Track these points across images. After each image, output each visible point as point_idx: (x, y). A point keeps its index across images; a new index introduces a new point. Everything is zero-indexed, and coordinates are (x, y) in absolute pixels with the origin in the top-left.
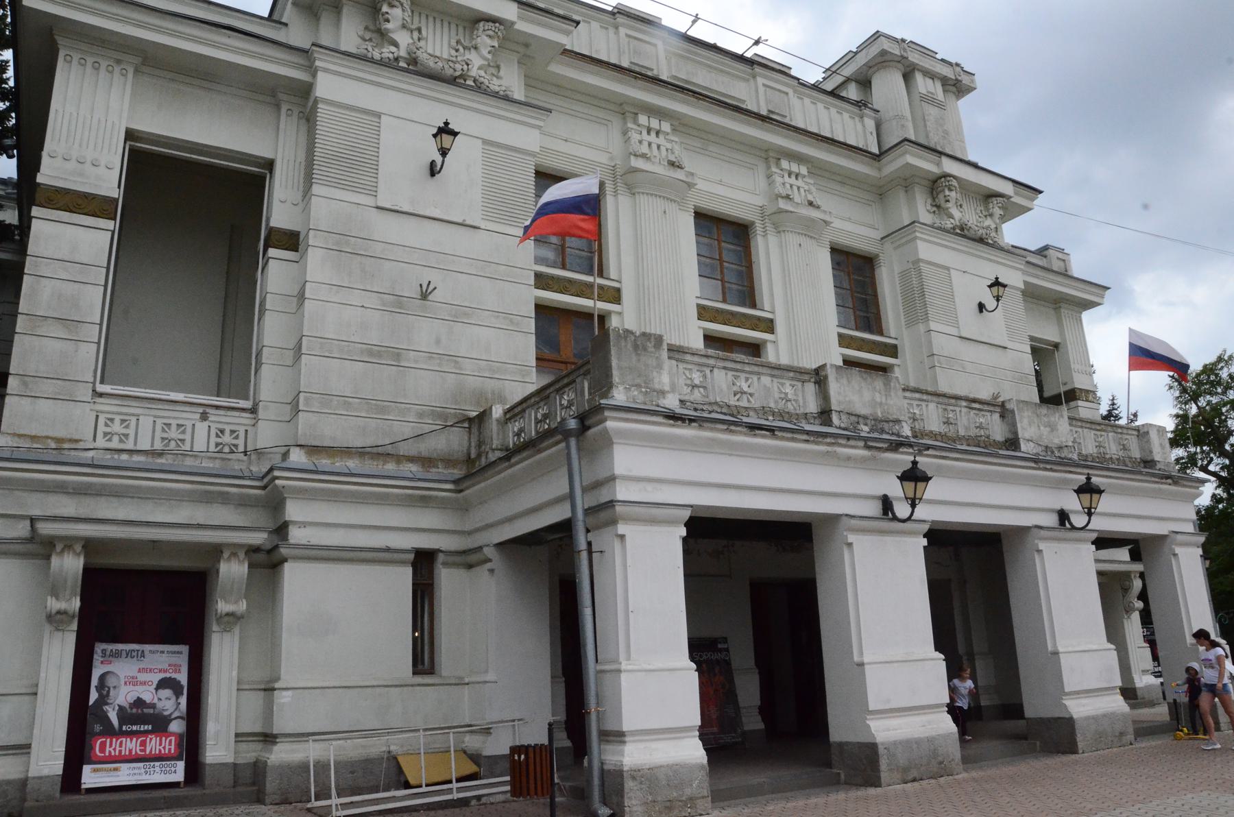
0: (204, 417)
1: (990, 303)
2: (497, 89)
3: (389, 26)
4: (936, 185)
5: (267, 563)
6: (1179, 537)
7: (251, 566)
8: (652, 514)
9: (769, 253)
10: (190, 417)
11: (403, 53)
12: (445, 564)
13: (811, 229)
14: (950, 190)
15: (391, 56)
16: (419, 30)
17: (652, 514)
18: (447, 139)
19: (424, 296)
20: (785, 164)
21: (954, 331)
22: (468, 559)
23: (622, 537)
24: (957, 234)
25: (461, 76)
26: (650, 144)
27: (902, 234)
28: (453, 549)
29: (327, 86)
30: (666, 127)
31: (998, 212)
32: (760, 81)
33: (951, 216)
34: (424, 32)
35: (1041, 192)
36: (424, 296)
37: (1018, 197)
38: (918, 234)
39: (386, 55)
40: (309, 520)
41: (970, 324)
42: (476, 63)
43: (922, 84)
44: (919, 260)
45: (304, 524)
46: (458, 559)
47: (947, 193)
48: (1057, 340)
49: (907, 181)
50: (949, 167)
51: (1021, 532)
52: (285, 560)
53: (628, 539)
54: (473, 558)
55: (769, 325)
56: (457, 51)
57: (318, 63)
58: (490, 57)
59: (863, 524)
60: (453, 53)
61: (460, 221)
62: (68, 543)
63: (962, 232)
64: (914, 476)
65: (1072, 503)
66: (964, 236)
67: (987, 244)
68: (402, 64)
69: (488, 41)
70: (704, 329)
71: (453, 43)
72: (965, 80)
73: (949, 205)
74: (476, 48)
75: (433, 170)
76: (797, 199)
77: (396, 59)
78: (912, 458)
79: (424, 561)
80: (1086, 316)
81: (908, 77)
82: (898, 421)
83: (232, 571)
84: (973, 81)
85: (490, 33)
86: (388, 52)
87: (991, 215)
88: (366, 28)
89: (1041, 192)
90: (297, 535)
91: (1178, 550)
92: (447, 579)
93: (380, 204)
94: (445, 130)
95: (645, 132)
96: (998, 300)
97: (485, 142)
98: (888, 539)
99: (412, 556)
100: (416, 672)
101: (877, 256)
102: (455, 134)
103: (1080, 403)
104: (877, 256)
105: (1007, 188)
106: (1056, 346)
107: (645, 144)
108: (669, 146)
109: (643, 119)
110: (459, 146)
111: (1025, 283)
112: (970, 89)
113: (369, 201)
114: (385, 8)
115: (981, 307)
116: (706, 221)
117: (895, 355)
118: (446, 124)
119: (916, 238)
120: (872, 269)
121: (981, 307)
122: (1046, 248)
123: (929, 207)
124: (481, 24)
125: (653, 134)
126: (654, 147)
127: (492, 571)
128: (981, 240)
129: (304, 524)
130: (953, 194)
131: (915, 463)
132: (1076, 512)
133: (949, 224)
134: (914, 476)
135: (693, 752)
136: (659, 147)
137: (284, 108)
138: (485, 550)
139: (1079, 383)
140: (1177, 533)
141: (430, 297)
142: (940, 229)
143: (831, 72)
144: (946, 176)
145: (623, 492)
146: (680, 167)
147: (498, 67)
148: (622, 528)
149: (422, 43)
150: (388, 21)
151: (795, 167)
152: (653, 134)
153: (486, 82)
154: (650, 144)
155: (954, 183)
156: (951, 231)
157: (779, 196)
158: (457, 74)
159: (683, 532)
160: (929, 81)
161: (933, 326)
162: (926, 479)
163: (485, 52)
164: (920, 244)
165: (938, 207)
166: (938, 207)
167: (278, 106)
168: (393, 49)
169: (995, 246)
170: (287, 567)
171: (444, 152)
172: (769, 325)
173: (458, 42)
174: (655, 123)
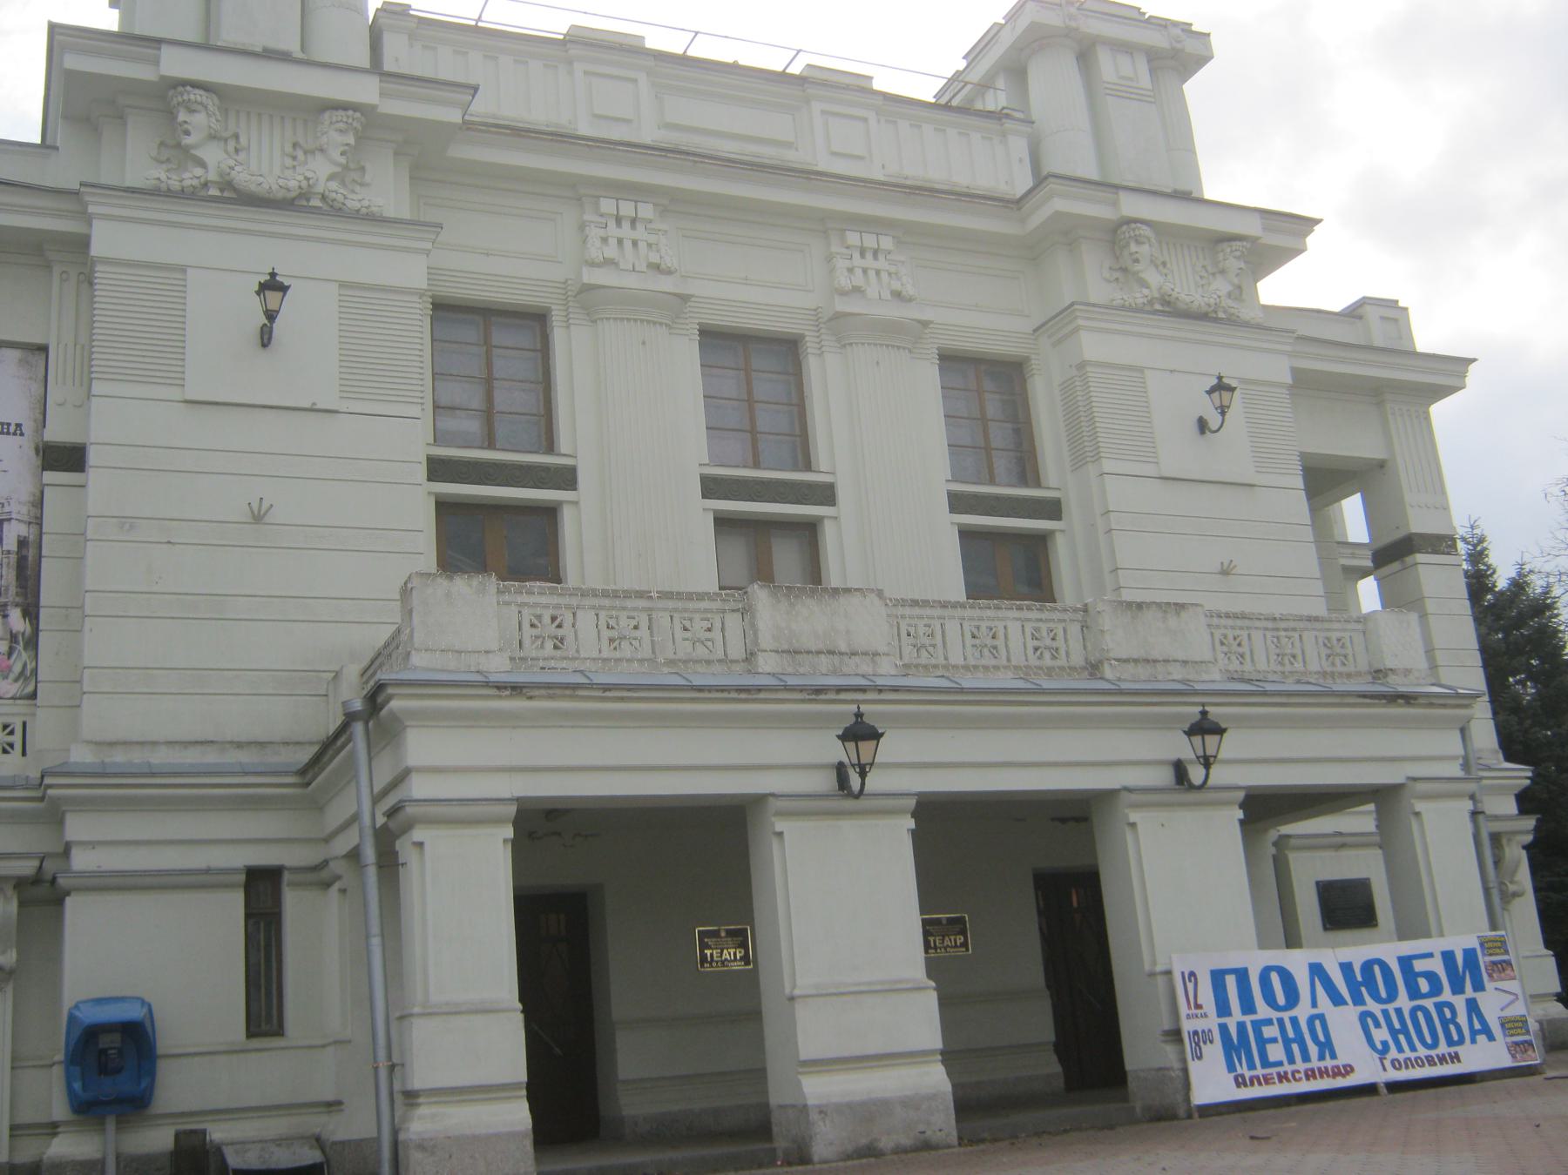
1: (1214, 420)
2: (357, 205)
3: (187, 141)
4: (1116, 235)
6: (1421, 787)
7: (21, 904)
8: (462, 815)
9: (830, 380)
11: (212, 176)
12: (295, 885)
13: (899, 335)
14: (1138, 243)
15: (195, 182)
16: (236, 137)
17: (462, 815)
18: (273, 297)
19: (258, 518)
20: (853, 238)
21: (1149, 470)
22: (319, 877)
23: (420, 845)
24: (1156, 312)
25: (300, 196)
26: (620, 241)
27: (1060, 323)
28: (303, 864)
29: (106, 240)
30: (646, 211)
31: (1233, 264)
32: (817, 107)
33: (1144, 284)
34: (243, 140)
35: (1317, 222)
36: (258, 518)
37: (1282, 234)
38: (1080, 322)
39: (187, 183)
40: (96, 843)
41: (1179, 452)
42: (320, 171)
43: (1108, 66)
44: (1082, 366)
45: (93, 845)
46: (311, 877)
47: (1133, 247)
48: (1379, 454)
49: (1067, 233)
50: (1131, 206)
51: (1105, 798)
52: (68, 894)
53: (427, 847)
54: (325, 874)
55: (826, 494)
56: (294, 158)
57: (91, 209)
58: (343, 160)
59: (805, 807)
60: (289, 162)
61: (307, 405)
63: (1170, 309)
64: (860, 732)
65: (1184, 748)
66: (1169, 314)
67: (1216, 320)
68: (214, 192)
69: (340, 139)
70: (715, 511)
71: (289, 149)
72: (1190, 46)
73: (1137, 267)
74: (322, 150)
75: (266, 338)
76: (872, 292)
77: (205, 185)
78: (854, 708)
80: (1440, 411)
81: (1085, 55)
84: (1208, 47)
85: (341, 125)
86: (191, 177)
87: (1223, 272)
88: (162, 144)
90: (81, 861)
91: (1419, 806)
92: (294, 903)
93: (188, 398)
94: (272, 285)
95: (612, 223)
96: (1223, 413)
97: (343, 285)
98: (847, 826)
99: (242, 878)
100: (250, 1034)
101: (1028, 359)
102: (284, 289)
103: (1420, 557)
104: (1028, 359)
105: (1252, 228)
106: (1381, 465)
107: (613, 242)
108: (652, 239)
109: (607, 206)
110: (290, 309)
111: (1295, 372)
112: (1203, 59)
113: (176, 393)
114: (182, 116)
115: (1202, 425)
116: (719, 342)
117: (1059, 518)
118: (273, 275)
119: (1076, 330)
120: (1023, 382)
121: (1202, 425)
122: (1364, 302)
123: (1107, 276)
124: (327, 115)
125: (626, 225)
126: (628, 245)
127: (343, 891)
128: (1203, 316)
129: (93, 845)
130: (1145, 249)
131: (859, 715)
132: (1191, 762)
133: (1139, 296)
134: (860, 732)
135: (517, 1115)
136: (635, 243)
137: (57, 270)
138: (332, 864)
139: (1420, 523)
140: (1415, 779)
141: (266, 519)
142: (1123, 308)
143: (973, 56)
144: (1130, 221)
145: (419, 788)
146: (669, 272)
147: (363, 169)
148: (418, 834)
149: (242, 156)
150: (187, 133)
151: (870, 241)
152: (626, 225)
153: (340, 198)
154: (620, 241)
155: (1145, 231)
156: (1146, 309)
157: (843, 293)
158: (293, 194)
159: (509, 832)
160: (1124, 62)
161: (1107, 466)
162: (875, 736)
163: (335, 154)
164: (1084, 337)
165: (1124, 270)
166: (1124, 270)
167: (48, 267)
168: (199, 171)
169: (1233, 321)
170: (69, 901)
171: (271, 316)
172: (826, 494)
173: (295, 145)
174: (627, 209)
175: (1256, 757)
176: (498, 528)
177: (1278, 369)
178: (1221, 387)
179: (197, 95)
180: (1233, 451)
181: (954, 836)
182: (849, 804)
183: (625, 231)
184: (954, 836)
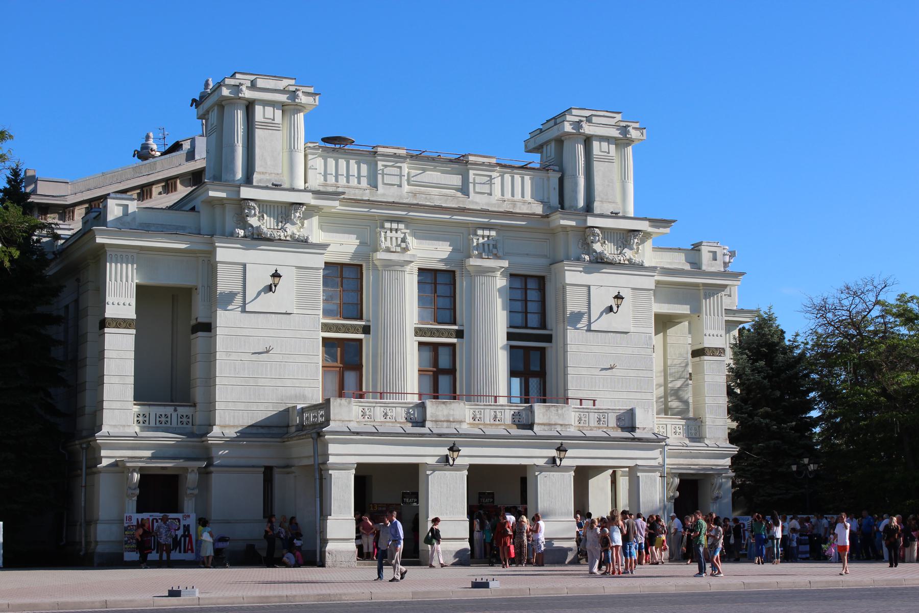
0: (175, 410)
5: (205, 473)
10: (169, 410)
18: (277, 279)
30: (401, 226)
62: (134, 469)
65: (553, 453)
79: (268, 471)
82: (461, 422)
83: (192, 478)
89: (674, 221)
92: (277, 477)
102: (280, 276)
103: (706, 358)
109: (387, 225)
155: (597, 230)
174: (395, 226)
175: (576, 457)
176: (346, 361)
177: (649, 282)
178: (618, 297)
179: (252, 204)
180: (622, 319)
181: (478, 476)
182: (448, 467)
183: (394, 234)
184: (478, 476)
